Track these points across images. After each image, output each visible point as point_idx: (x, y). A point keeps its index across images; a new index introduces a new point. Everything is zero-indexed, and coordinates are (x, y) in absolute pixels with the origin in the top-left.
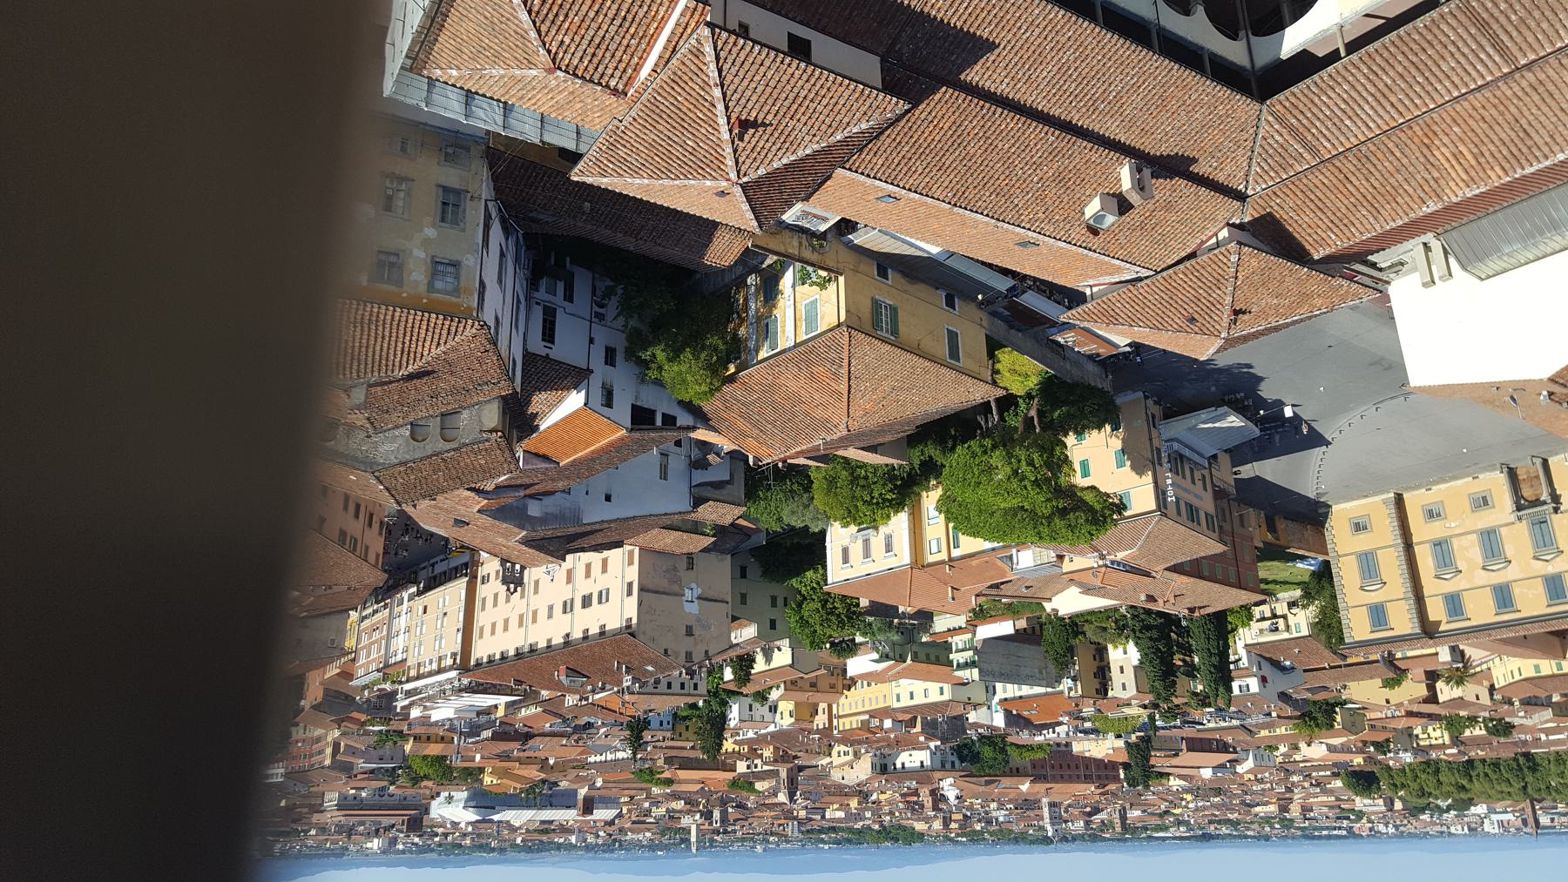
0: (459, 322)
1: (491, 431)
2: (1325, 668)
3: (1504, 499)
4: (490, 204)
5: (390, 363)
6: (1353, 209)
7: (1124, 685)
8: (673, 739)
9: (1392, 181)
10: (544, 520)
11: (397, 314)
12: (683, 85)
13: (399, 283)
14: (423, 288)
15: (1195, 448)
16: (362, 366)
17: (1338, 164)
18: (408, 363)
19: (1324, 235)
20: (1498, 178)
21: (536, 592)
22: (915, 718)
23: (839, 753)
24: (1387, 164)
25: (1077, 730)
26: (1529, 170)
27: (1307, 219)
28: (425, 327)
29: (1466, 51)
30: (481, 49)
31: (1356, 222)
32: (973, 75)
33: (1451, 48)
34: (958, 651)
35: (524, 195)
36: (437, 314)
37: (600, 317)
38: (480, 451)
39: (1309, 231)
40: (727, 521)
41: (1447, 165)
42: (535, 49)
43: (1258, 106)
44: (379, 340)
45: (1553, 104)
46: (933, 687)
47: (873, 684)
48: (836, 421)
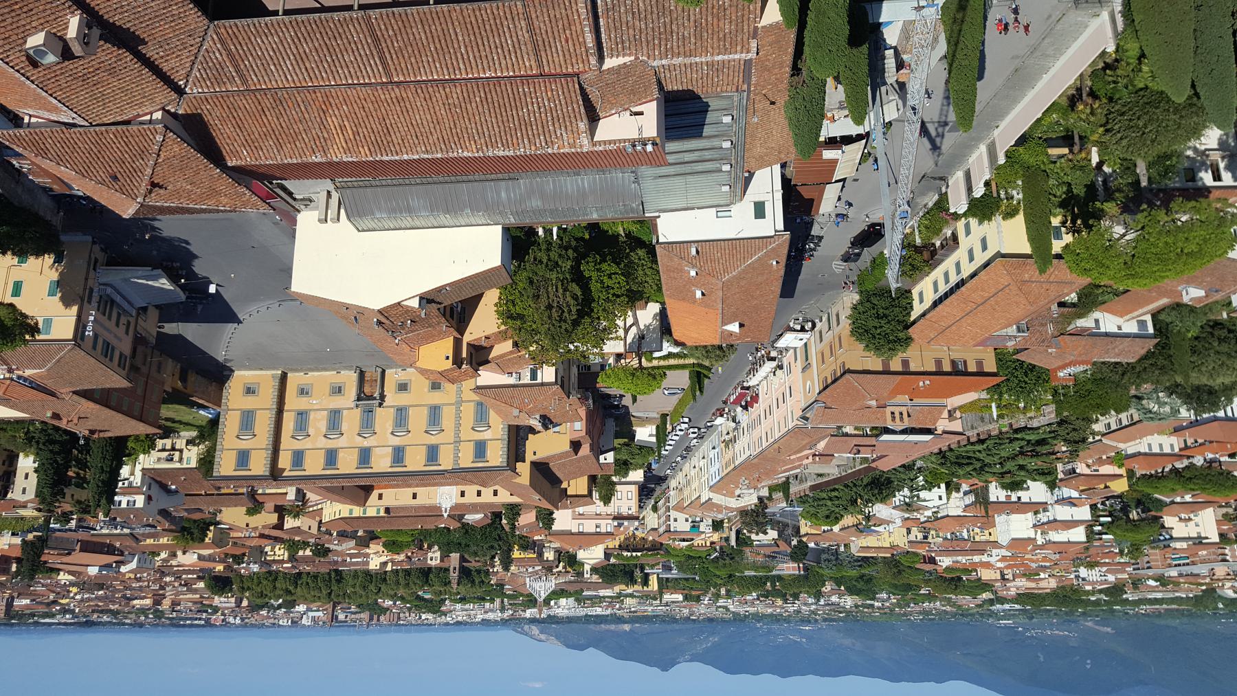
2: (201, 495)
3: (352, 391)
6: (263, 137)
9: (295, 127)
17: (259, 97)
19: (238, 149)
20: (365, 156)
24: (294, 112)
26: (385, 158)
27: (227, 131)
29: (362, 53)
31: (264, 148)
33: (353, 46)
39: (228, 141)
41: (334, 132)
43: (206, 21)
45: (407, 118)
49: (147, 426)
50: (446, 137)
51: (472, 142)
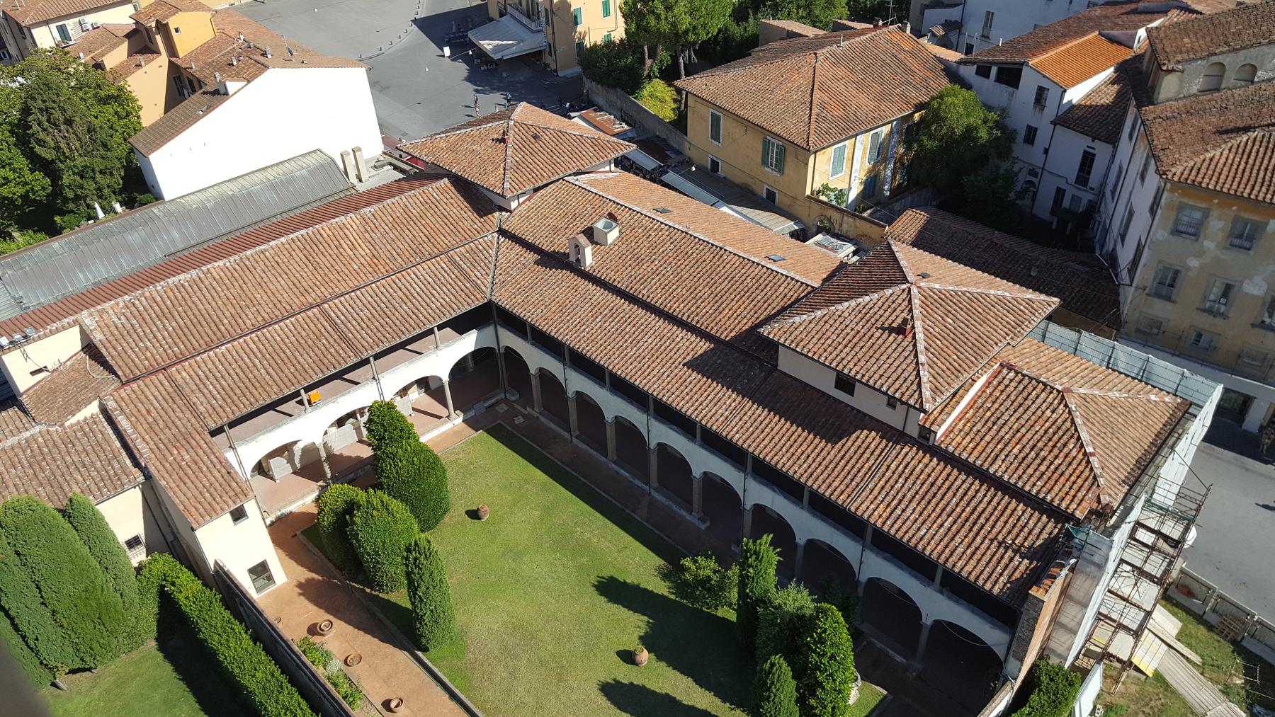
0: (1186, 179)
1: (1173, 71)
4: (1127, 281)
5: (1264, 144)
6: (422, 215)
9: (397, 234)
11: (1248, 191)
12: (951, 367)
13: (1236, 220)
14: (1215, 213)
17: (435, 250)
18: (1247, 143)
19: (441, 196)
20: (324, 228)
24: (402, 247)
26: (303, 232)
27: (455, 211)
29: (354, 322)
30: (1126, 414)
31: (420, 205)
32: (703, 346)
33: (364, 325)
35: (1091, 287)
36: (1208, 188)
37: (1033, 173)
38: (1188, 52)
39: (452, 201)
41: (360, 241)
42: (1079, 409)
43: (493, 298)
45: (293, 278)
48: (826, 64)
50: (247, 272)
51: (217, 277)
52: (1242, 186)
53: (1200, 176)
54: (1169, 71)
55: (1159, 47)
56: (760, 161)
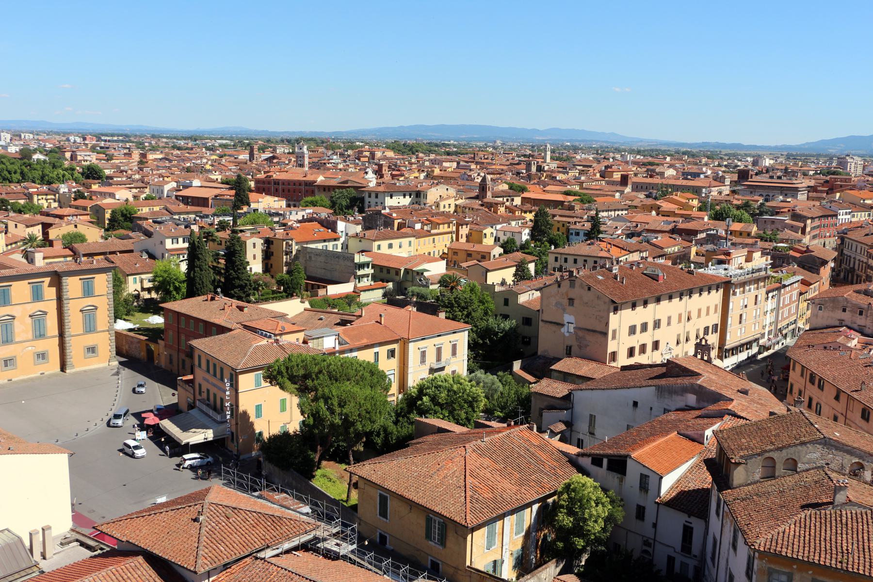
2: (121, 252)
7: (254, 247)
8: (569, 223)
10: (684, 390)
11: (817, 558)
15: (204, 415)
16: (839, 519)
21: (679, 335)
22: (398, 229)
23: (449, 207)
25: (283, 215)
28: (795, 546)
34: (367, 276)
37: (646, 543)
38: (746, 449)
40: (545, 382)
44: (828, 538)
46: (385, 250)
47: (426, 254)
49: (173, 309)
52: (812, 554)
53: (780, 546)
54: (738, 464)
55: (726, 445)
56: (424, 535)
